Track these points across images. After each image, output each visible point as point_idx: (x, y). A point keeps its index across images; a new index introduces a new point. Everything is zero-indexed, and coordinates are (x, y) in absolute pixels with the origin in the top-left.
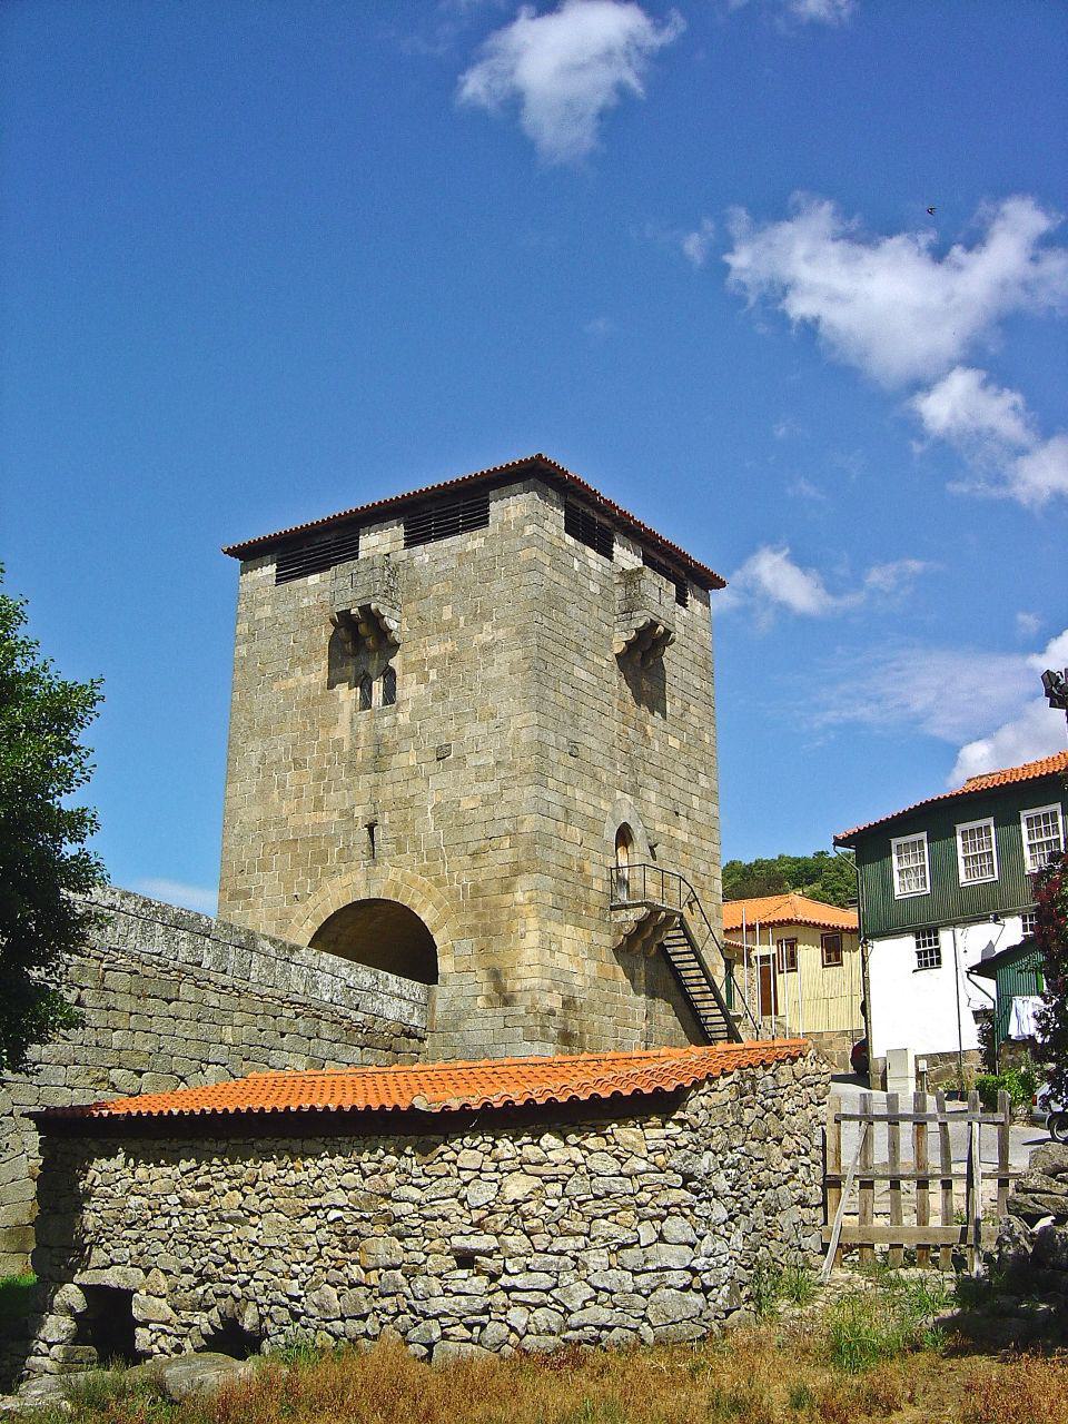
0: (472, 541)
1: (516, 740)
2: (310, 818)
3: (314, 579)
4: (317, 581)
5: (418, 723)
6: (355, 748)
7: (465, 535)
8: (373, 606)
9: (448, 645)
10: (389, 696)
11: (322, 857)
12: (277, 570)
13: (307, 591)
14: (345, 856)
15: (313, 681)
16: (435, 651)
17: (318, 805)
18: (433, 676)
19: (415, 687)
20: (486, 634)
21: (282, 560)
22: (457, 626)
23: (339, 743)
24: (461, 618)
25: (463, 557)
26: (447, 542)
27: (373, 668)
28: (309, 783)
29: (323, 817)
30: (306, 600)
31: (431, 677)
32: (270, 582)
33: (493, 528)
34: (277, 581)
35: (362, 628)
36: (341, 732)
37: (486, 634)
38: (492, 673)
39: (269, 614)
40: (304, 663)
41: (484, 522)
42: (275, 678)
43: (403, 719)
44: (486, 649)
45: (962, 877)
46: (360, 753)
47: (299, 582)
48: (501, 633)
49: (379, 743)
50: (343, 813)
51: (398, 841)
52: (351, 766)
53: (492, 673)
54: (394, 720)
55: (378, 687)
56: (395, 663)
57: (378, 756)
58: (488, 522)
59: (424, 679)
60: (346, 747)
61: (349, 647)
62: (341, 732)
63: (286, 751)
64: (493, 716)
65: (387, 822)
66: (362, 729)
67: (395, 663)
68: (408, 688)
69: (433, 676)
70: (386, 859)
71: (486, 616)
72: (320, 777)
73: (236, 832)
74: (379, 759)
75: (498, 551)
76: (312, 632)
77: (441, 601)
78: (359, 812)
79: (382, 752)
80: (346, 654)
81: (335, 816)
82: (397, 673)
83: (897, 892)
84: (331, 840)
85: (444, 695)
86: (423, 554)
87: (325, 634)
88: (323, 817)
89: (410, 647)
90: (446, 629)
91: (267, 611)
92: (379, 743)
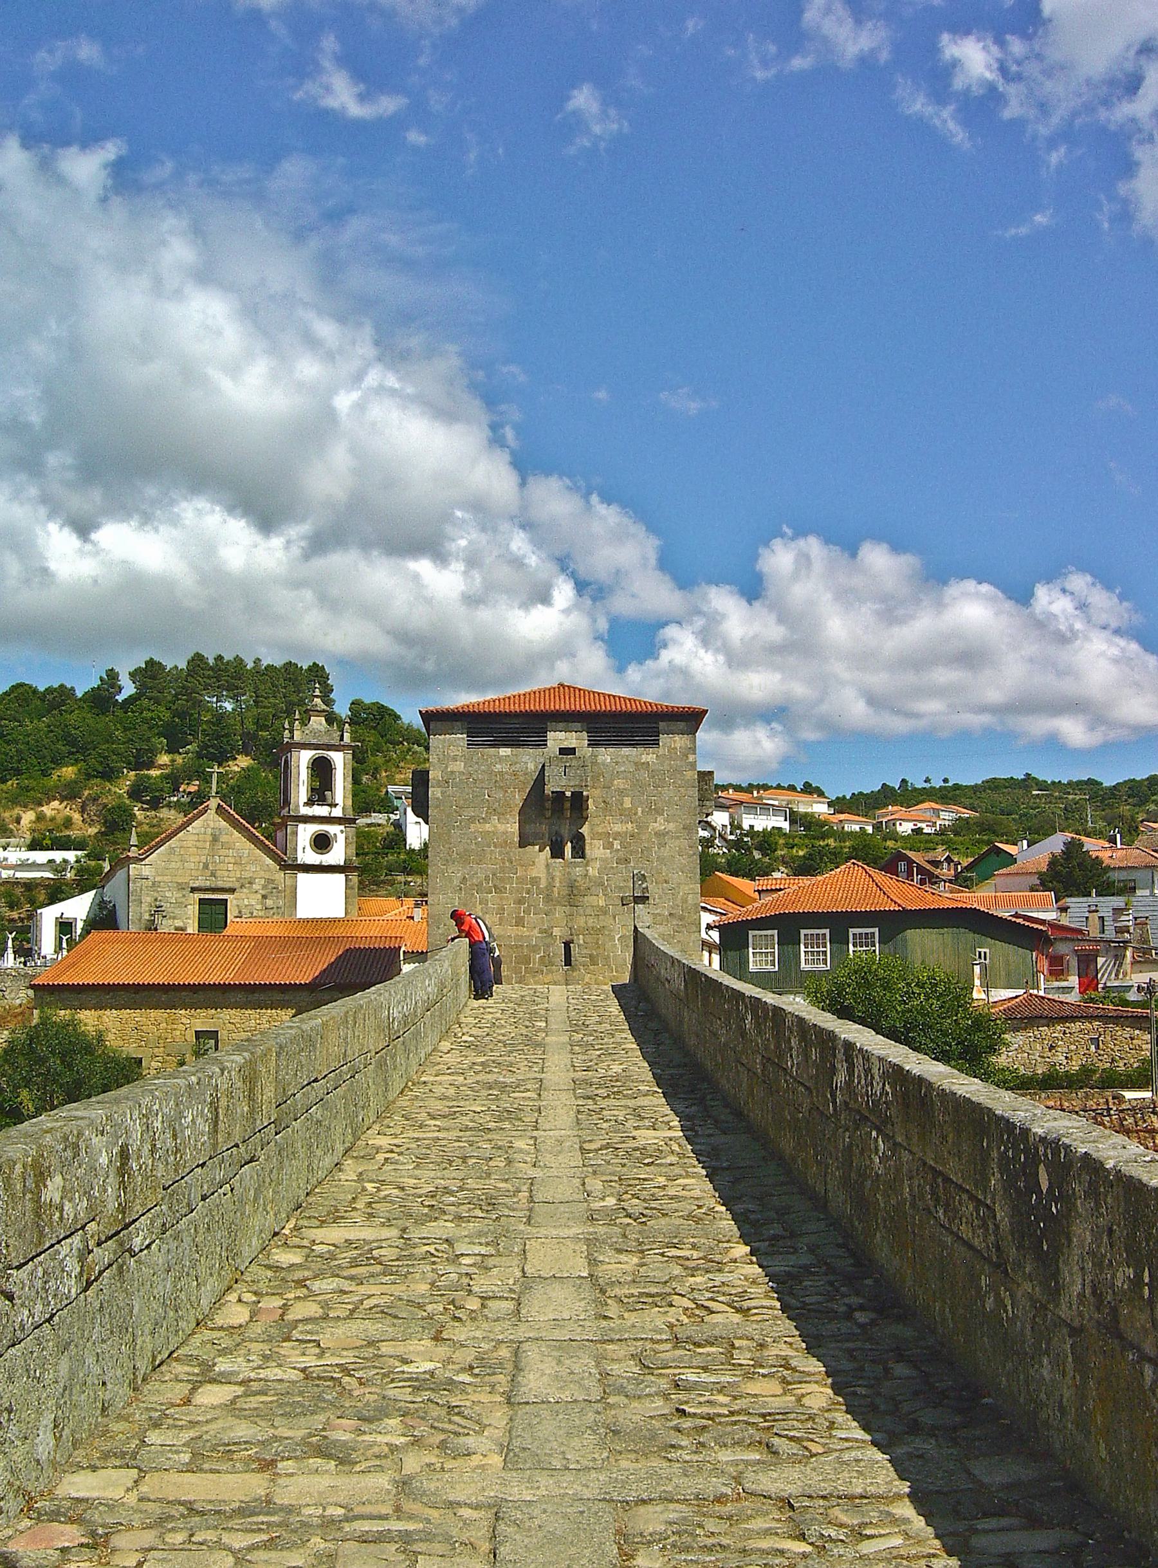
0: (648, 756)
1: (685, 901)
2: (512, 931)
3: (504, 751)
4: (509, 753)
6: (550, 886)
8: (585, 793)
9: (630, 825)
10: (579, 851)
11: (527, 960)
13: (501, 759)
14: (547, 961)
16: (618, 828)
17: (520, 922)
18: (617, 845)
20: (659, 824)
22: (635, 814)
23: (535, 881)
25: (639, 765)
26: (626, 751)
27: (565, 831)
29: (524, 931)
33: (661, 751)
37: (659, 824)
38: (665, 852)
39: (462, 770)
40: (501, 815)
41: (656, 743)
42: (472, 820)
43: (592, 871)
44: (658, 834)
45: (803, 965)
48: (671, 826)
49: (572, 886)
51: (591, 956)
52: (548, 899)
53: (665, 852)
56: (585, 830)
59: (610, 846)
61: (548, 814)
63: (487, 878)
64: (666, 882)
65: (581, 942)
67: (585, 830)
68: (595, 849)
69: (617, 845)
71: (659, 812)
72: (520, 902)
73: (440, 931)
74: (573, 894)
78: (556, 932)
81: (536, 931)
83: (751, 967)
84: (534, 949)
85: (627, 861)
86: (606, 755)
87: (518, 799)
88: (524, 931)
89: (597, 821)
90: (627, 815)
92: (572, 886)
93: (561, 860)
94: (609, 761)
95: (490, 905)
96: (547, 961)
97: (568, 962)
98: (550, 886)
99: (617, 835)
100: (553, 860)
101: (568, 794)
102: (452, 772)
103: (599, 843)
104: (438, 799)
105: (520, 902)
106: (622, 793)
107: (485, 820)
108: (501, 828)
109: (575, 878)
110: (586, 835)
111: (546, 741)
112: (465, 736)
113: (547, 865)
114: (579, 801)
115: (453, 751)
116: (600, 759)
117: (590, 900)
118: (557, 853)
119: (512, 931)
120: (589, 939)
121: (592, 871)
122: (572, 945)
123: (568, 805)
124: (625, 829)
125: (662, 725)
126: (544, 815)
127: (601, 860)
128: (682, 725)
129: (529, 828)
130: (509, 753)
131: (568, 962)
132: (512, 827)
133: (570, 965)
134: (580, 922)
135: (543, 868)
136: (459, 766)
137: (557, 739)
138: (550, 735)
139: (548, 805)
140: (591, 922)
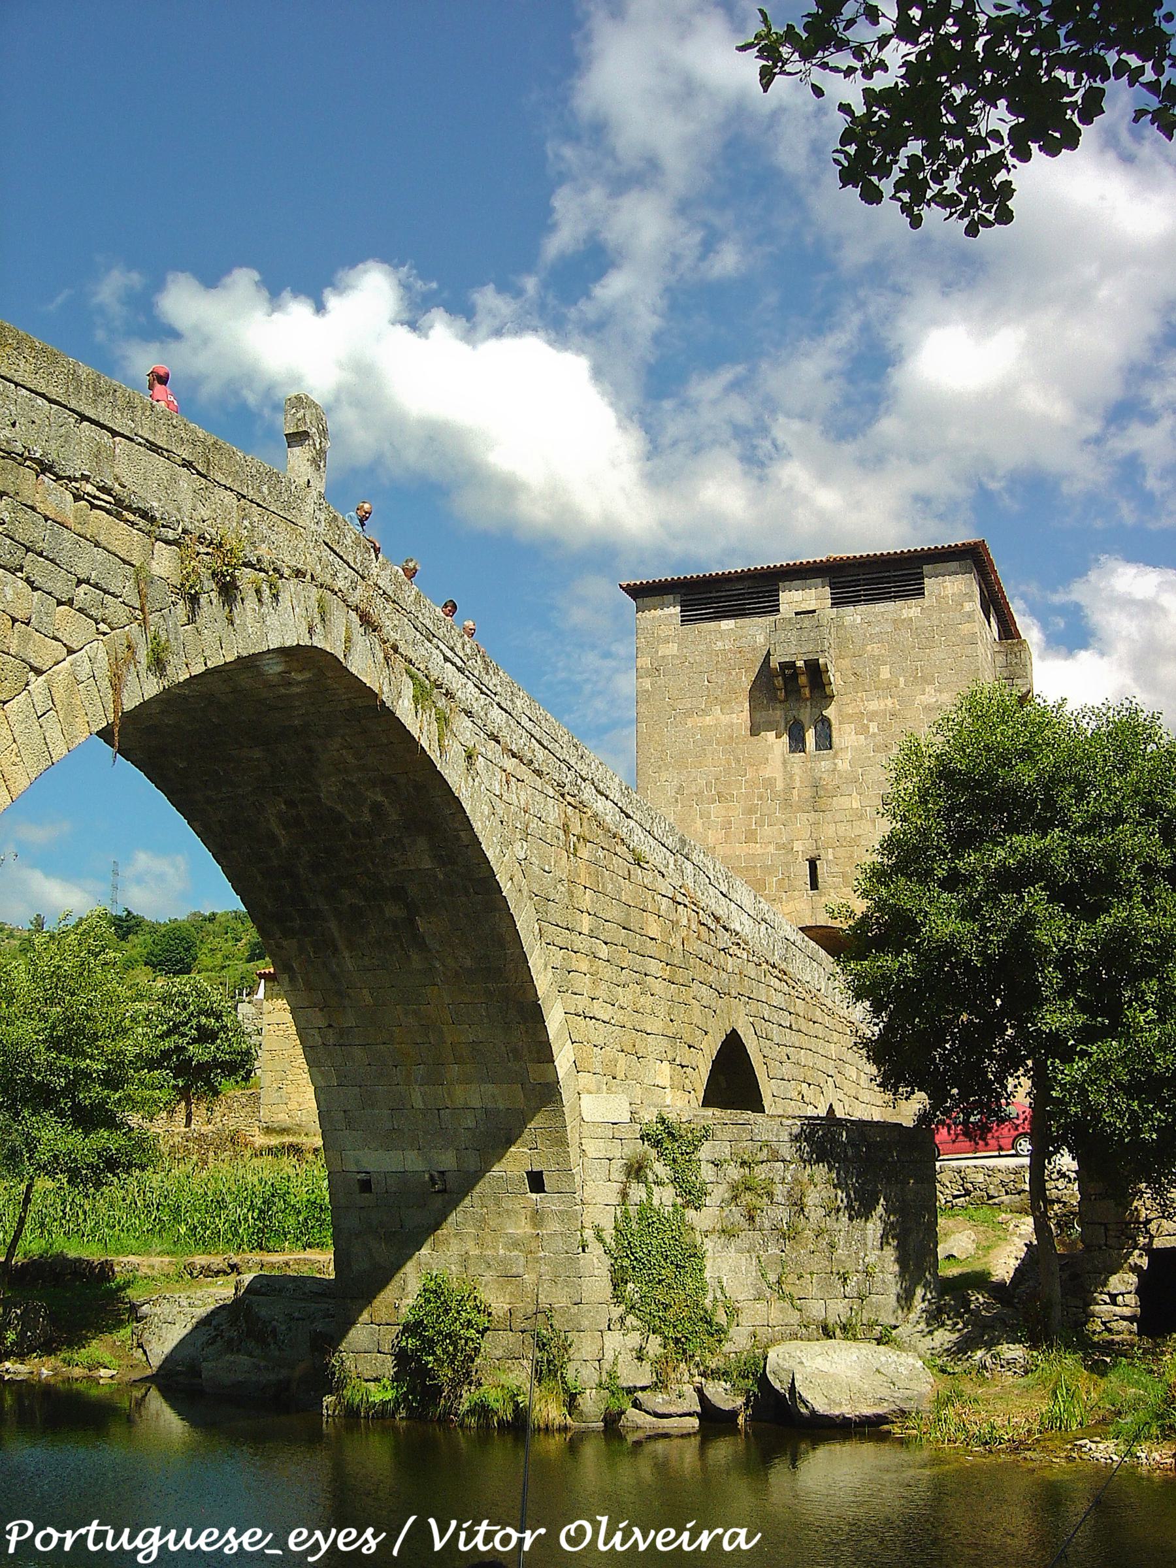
0: (909, 610)
2: (741, 849)
3: (727, 624)
4: (733, 626)
5: (860, 771)
6: (789, 788)
7: (900, 603)
8: (821, 661)
9: (889, 701)
10: (825, 741)
12: (681, 611)
14: (786, 885)
15: (735, 721)
16: (873, 706)
17: (750, 837)
18: (873, 728)
19: (854, 737)
21: (684, 601)
23: (769, 783)
24: (901, 679)
26: (880, 607)
27: (805, 715)
28: (736, 811)
29: (757, 849)
30: (719, 644)
31: (871, 730)
32: (675, 622)
33: (926, 602)
34: (682, 621)
35: (803, 680)
36: (773, 770)
39: (675, 652)
40: (724, 703)
41: (920, 593)
42: (688, 713)
43: (843, 765)
46: (795, 792)
47: (712, 625)
50: (779, 847)
52: (787, 803)
54: (833, 766)
55: (810, 736)
56: (830, 712)
57: (816, 797)
58: (923, 594)
59: (863, 730)
60: (780, 785)
61: (781, 695)
62: (773, 770)
65: (831, 857)
66: (797, 770)
67: (830, 712)
68: (845, 736)
69: (873, 728)
70: (832, 890)
71: (927, 680)
72: (750, 811)
75: (936, 622)
76: (730, 674)
77: (878, 661)
78: (798, 846)
79: (821, 793)
80: (773, 699)
81: (771, 849)
82: (833, 722)
84: (768, 869)
86: (854, 615)
87: (746, 681)
88: (757, 849)
89: (846, 699)
90: (888, 689)
91: (672, 649)
93: (802, 754)
94: (859, 621)
95: (713, 818)
96: (786, 885)
97: (814, 885)
98: (789, 788)
99: (872, 716)
100: (791, 755)
101: (800, 664)
102: (663, 657)
103: (849, 728)
104: (647, 691)
105: (750, 811)
106: (878, 661)
107: (705, 712)
108: (725, 719)
109: (819, 775)
110: (832, 718)
111: (778, 605)
112: (678, 608)
113: (784, 763)
114: (816, 672)
115: (665, 631)
116: (848, 621)
117: (840, 802)
118: (797, 744)
119: (741, 849)
120: (841, 852)
121: (843, 765)
122: (818, 862)
123: (803, 680)
124: (882, 707)
125: (927, 569)
126: (776, 699)
127: (856, 749)
128: (954, 565)
129: (761, 716)
130: (733, 626)
131: (814, 885)
132: (741, 716)
133: (817, 889)
134: (830, 831)
135: (778, 763)
136: (672, 649)
137: (792, 599)
138: (784, 596)
139: (779, 682)
140: (842, 829)
